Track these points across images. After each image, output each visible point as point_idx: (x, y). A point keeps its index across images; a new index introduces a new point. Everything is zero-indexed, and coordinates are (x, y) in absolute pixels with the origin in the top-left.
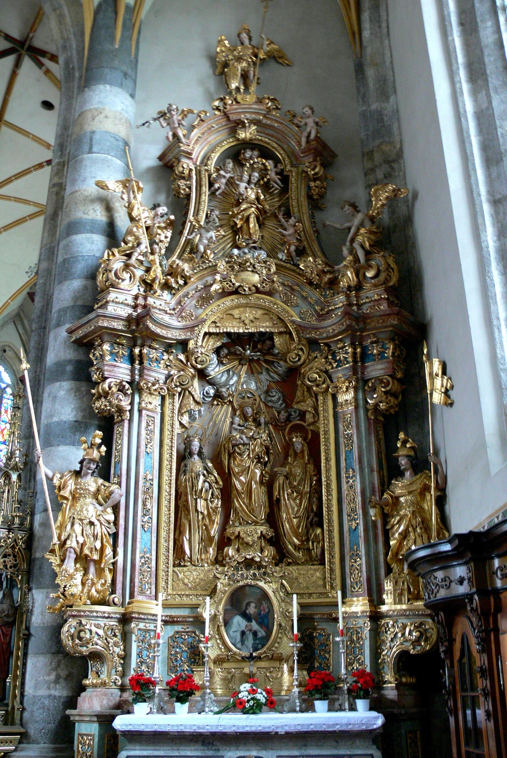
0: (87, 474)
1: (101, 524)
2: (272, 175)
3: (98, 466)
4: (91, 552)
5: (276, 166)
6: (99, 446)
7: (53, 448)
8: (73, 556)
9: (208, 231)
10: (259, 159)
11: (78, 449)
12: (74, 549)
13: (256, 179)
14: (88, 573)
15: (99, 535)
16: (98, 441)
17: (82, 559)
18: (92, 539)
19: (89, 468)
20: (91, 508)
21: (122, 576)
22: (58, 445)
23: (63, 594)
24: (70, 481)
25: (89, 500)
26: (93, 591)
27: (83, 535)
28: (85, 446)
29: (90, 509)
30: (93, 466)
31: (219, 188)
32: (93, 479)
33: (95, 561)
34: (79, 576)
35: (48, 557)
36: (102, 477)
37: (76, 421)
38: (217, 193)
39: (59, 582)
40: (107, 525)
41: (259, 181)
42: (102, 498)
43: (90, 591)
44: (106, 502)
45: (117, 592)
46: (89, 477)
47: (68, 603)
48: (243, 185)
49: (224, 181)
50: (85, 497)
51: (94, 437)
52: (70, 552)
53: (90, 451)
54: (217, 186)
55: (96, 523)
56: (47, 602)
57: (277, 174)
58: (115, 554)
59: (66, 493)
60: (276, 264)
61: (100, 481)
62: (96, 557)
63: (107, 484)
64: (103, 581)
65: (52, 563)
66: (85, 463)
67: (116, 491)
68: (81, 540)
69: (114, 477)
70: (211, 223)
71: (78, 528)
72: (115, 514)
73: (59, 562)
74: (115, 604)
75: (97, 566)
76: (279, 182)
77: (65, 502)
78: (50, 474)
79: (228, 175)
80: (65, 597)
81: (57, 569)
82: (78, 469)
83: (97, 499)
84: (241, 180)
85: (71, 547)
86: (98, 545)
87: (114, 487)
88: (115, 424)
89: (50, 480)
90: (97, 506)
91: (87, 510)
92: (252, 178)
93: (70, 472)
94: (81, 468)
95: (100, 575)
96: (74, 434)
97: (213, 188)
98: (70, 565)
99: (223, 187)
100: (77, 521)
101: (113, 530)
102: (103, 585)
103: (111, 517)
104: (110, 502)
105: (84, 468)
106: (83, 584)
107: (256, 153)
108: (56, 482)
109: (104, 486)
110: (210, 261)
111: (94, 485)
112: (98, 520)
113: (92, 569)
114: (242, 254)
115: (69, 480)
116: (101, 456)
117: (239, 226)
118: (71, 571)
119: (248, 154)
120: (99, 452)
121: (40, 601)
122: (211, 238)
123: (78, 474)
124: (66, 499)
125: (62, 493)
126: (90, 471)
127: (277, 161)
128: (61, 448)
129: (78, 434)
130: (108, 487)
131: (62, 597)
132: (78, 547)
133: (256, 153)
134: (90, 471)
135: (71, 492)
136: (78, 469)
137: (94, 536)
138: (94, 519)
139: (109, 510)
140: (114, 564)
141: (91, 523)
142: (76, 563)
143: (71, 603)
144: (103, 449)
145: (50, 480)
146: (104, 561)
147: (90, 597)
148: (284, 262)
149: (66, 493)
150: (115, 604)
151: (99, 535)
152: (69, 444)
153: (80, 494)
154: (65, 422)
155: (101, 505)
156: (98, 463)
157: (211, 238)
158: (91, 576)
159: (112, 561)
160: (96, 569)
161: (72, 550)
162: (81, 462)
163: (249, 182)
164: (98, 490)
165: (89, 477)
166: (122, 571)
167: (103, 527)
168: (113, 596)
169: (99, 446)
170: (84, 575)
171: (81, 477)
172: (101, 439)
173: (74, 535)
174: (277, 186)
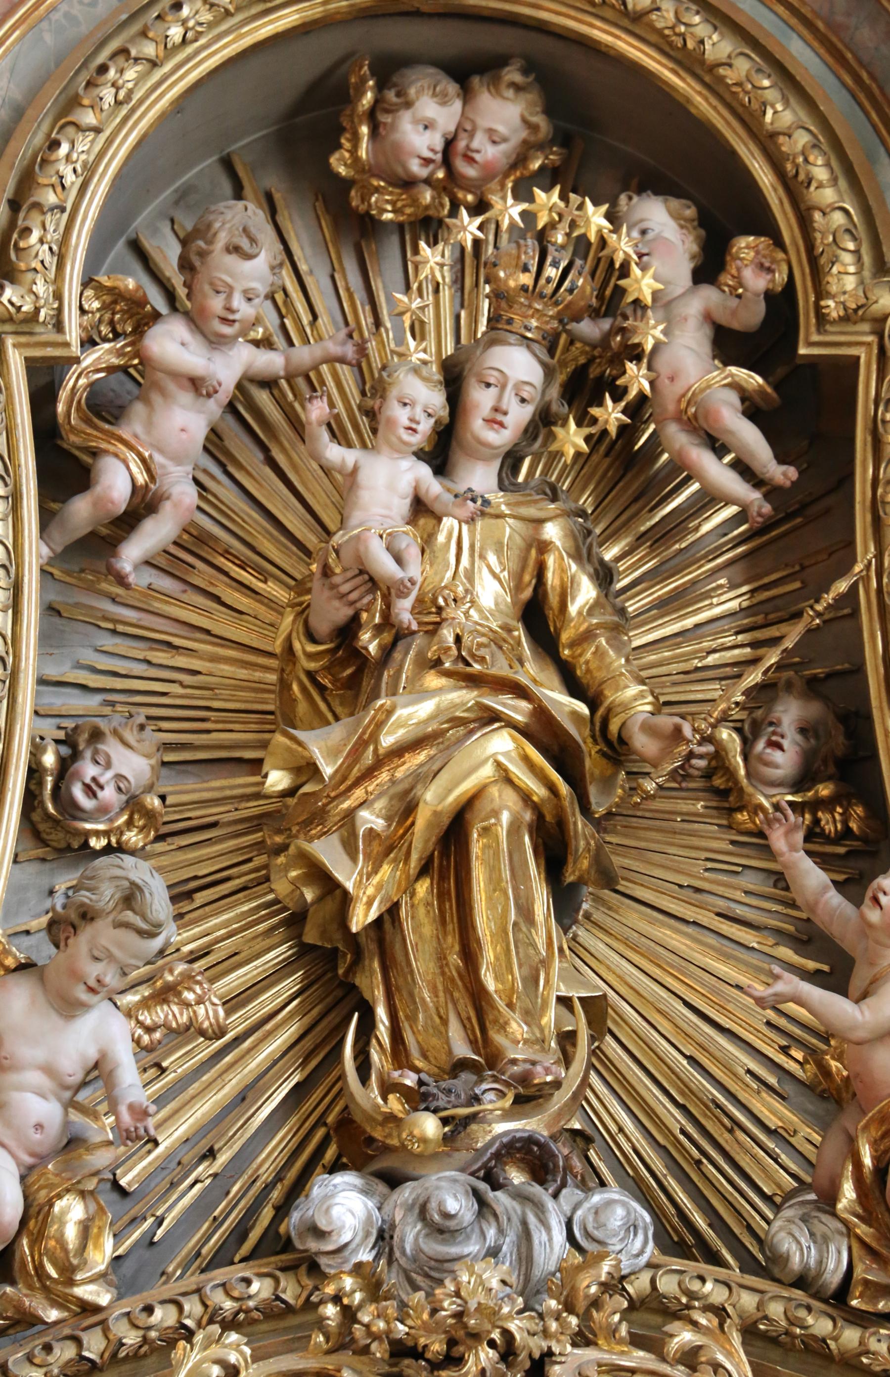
2: (681, 356)
5: (709, 268)
9: (69, 1008)
10: (547, 200)
13: (519, 415)
31: (144, 505)
38: (132, 553)
41: (544, 422)
48: (389, 479)
49: (185, 423)
54: (116, 481)
57: (728, 344)
60: (751, 1333)
70: (102, 933)
76: (751, 438)
79: (228, 368)
84: (366, 421)
92: (481, 399)
97: (81, 510)
99: (184, 494)
107: (504, 117)
110: (88, 1309)
114: (410, 1235)
117: (361, 918)
119: (424, 123)
122: (99, 1071)
127: (725, 214)
133: (504, 117)
148: (838, 1299)
157: (99, 1071)
163: (442, 450)
174: (728, 474)
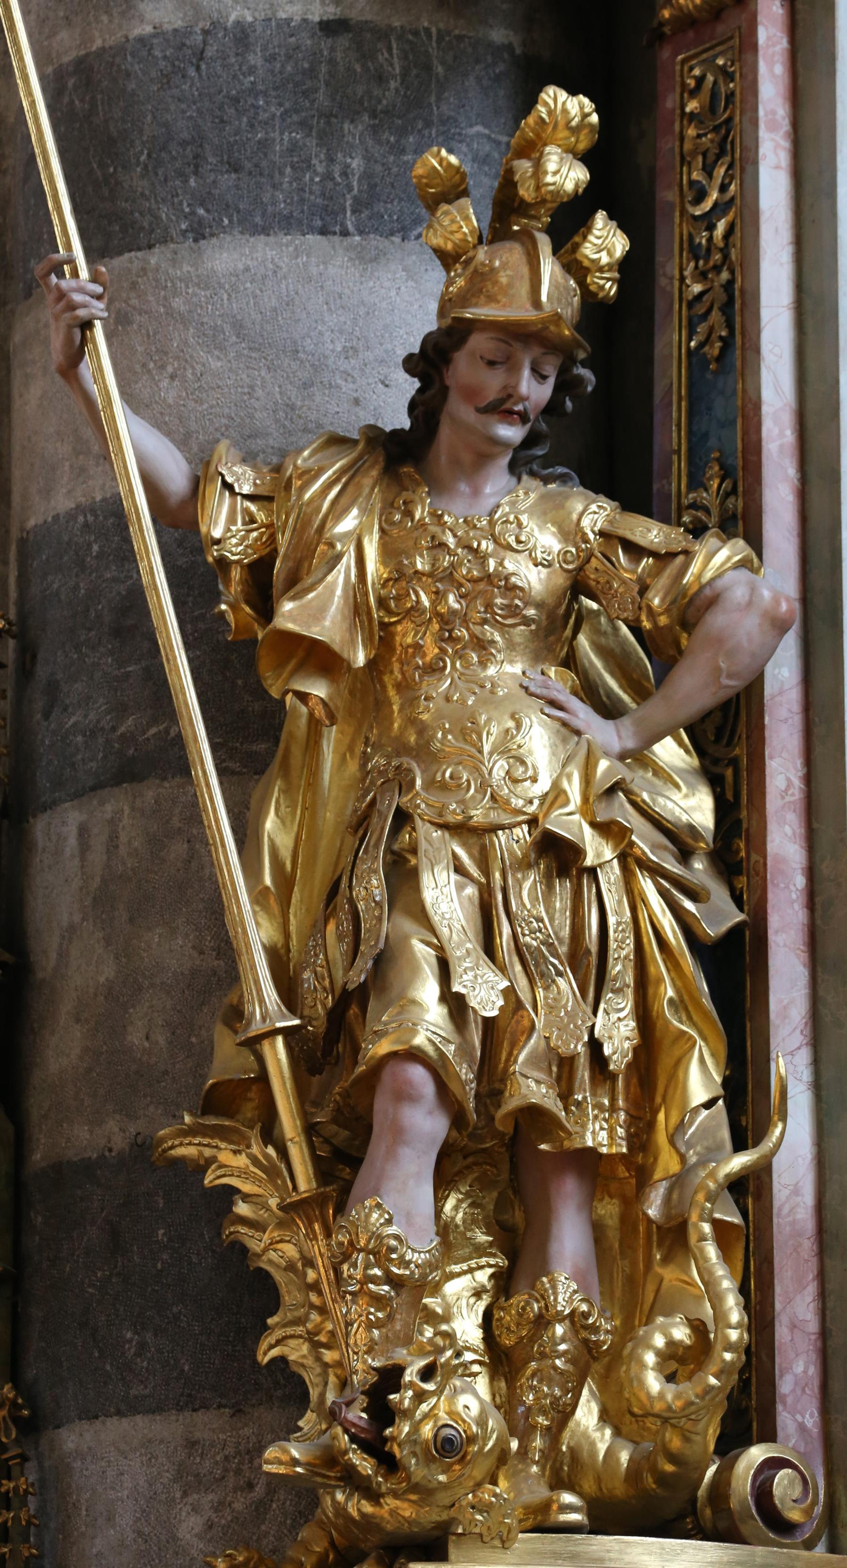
0: (483, 453)
1: (628, 859)
3: (566, 385)
4: (565, 1096)
6: (568, 221)
7: (155, 257)
8: (425, 1125)
11: (368, 260)
12: (437, 1068)
14: (543, 1267)
15: (621, 949)
16: (567, 175)
17: (503, 1162)
18: (566, 985)
19: (502, 407)
20: (538, 740)
21: (811, 1290)
22: (199, 232)
23: (375, 1446)
24: (349, 523)
25: (508, 669)
26: (587, 1414)
27: (489, 948)
28: (464, 220)
29: (532, 751)
30: (535, 391)
32: (530, 493)
33: (588, 1162)
34: (462, 1305)
35: (187, 1151)
36: (599, 482)
37: (329, 28)
39: (297, 1352)
40: (672, 866)
42: (625, 651)
43: (564, 1414)
44: (641, 693)
45: (786, 1421)
46: (497, 481)
47: (398, 1511)
50: (482, 645)
51: (532, 149)
52: (405, 1095)
53: (507, 259)
55: (597, 850)
56: (190, 1526)
58: (747, 1104)
59: (319, 611)
61: (595, 514)
62: (600, 1134)
63: (652, 533)
64: (681, 1333)
65: (230, 1192)
66: (464, 368)
67: (738, 587)
68: (485, 993)
69: (696, 482)
71: (445, 896)
72: (715, 782)
73: (305, 1180)
74: (779, 1525)
75: (609, 1210)
77: (319, 690)
78: (176, 473)
80: (389, 1463)
81: (277, 1251)
82: (399, 419)
83: (570, 661)
85: (414, 1055)
86: (618, 1032)
87: (716, 559)
88: (658, 36)
89: (178, 518)
90: (583, 714)
91: (507, 748)
93: (337, 441)
94: (427, 409)
95: (633, 1285)
96: (329, 139)
98: (406, 1201)
100: (429, 836)
101: (719, 916)
102: (679, 1362)
103: (696, 808)
104: (694, 687)
105: (460, 410)
106: (502, 1359)
108: (225, 525)
109: (635, 550)
111: (548, 541)
112: (607, 829)
113: (570, 1239)
115: (338, 511)
116: (587, 294)
118: (420, 1249)
120: (575, 268)
121: (126, 1519)
123: (402, 457)
124: (320, 658)
125: (289, 614)
126: (511, 433)
128: (229, 257)
129: (353, 131)
130: (663, 558)
131: (364, 1464)
132: (464, 1050)
134: (511, 433)
135: (357, 608)
136: (399, 419)
137: (576, 957)
138: (569, 822)
139: (670, 752)
140: (750, 1189)
141: (557, 856)
142: (443, 1182)
143: (432, 1516)
144: (606, 242)
145: (178, 518)
146: (667, 1162)
147: (565, 1470)
149: (319, 611)
150: (779, 1525)
151: (621, 949)
152: (288, 223)
153: (446, 620)
154: (242, 36)
155: (609, 710)
156: (566, 355)
158: (565, 1291)
159: (738, 1162)
160: (598, 1230)
161: (418, 1074)
162: (431, 362)
164: (578, 586)
165: (497, 481)
166: (808, 1246)
167: (647, 886)
168: (757, 1453)
169: (568, 221)
170: (504, 1283)
171: (438, 487)
172: (586, 158)
173: (423, 952)
